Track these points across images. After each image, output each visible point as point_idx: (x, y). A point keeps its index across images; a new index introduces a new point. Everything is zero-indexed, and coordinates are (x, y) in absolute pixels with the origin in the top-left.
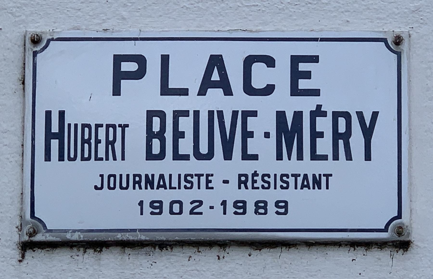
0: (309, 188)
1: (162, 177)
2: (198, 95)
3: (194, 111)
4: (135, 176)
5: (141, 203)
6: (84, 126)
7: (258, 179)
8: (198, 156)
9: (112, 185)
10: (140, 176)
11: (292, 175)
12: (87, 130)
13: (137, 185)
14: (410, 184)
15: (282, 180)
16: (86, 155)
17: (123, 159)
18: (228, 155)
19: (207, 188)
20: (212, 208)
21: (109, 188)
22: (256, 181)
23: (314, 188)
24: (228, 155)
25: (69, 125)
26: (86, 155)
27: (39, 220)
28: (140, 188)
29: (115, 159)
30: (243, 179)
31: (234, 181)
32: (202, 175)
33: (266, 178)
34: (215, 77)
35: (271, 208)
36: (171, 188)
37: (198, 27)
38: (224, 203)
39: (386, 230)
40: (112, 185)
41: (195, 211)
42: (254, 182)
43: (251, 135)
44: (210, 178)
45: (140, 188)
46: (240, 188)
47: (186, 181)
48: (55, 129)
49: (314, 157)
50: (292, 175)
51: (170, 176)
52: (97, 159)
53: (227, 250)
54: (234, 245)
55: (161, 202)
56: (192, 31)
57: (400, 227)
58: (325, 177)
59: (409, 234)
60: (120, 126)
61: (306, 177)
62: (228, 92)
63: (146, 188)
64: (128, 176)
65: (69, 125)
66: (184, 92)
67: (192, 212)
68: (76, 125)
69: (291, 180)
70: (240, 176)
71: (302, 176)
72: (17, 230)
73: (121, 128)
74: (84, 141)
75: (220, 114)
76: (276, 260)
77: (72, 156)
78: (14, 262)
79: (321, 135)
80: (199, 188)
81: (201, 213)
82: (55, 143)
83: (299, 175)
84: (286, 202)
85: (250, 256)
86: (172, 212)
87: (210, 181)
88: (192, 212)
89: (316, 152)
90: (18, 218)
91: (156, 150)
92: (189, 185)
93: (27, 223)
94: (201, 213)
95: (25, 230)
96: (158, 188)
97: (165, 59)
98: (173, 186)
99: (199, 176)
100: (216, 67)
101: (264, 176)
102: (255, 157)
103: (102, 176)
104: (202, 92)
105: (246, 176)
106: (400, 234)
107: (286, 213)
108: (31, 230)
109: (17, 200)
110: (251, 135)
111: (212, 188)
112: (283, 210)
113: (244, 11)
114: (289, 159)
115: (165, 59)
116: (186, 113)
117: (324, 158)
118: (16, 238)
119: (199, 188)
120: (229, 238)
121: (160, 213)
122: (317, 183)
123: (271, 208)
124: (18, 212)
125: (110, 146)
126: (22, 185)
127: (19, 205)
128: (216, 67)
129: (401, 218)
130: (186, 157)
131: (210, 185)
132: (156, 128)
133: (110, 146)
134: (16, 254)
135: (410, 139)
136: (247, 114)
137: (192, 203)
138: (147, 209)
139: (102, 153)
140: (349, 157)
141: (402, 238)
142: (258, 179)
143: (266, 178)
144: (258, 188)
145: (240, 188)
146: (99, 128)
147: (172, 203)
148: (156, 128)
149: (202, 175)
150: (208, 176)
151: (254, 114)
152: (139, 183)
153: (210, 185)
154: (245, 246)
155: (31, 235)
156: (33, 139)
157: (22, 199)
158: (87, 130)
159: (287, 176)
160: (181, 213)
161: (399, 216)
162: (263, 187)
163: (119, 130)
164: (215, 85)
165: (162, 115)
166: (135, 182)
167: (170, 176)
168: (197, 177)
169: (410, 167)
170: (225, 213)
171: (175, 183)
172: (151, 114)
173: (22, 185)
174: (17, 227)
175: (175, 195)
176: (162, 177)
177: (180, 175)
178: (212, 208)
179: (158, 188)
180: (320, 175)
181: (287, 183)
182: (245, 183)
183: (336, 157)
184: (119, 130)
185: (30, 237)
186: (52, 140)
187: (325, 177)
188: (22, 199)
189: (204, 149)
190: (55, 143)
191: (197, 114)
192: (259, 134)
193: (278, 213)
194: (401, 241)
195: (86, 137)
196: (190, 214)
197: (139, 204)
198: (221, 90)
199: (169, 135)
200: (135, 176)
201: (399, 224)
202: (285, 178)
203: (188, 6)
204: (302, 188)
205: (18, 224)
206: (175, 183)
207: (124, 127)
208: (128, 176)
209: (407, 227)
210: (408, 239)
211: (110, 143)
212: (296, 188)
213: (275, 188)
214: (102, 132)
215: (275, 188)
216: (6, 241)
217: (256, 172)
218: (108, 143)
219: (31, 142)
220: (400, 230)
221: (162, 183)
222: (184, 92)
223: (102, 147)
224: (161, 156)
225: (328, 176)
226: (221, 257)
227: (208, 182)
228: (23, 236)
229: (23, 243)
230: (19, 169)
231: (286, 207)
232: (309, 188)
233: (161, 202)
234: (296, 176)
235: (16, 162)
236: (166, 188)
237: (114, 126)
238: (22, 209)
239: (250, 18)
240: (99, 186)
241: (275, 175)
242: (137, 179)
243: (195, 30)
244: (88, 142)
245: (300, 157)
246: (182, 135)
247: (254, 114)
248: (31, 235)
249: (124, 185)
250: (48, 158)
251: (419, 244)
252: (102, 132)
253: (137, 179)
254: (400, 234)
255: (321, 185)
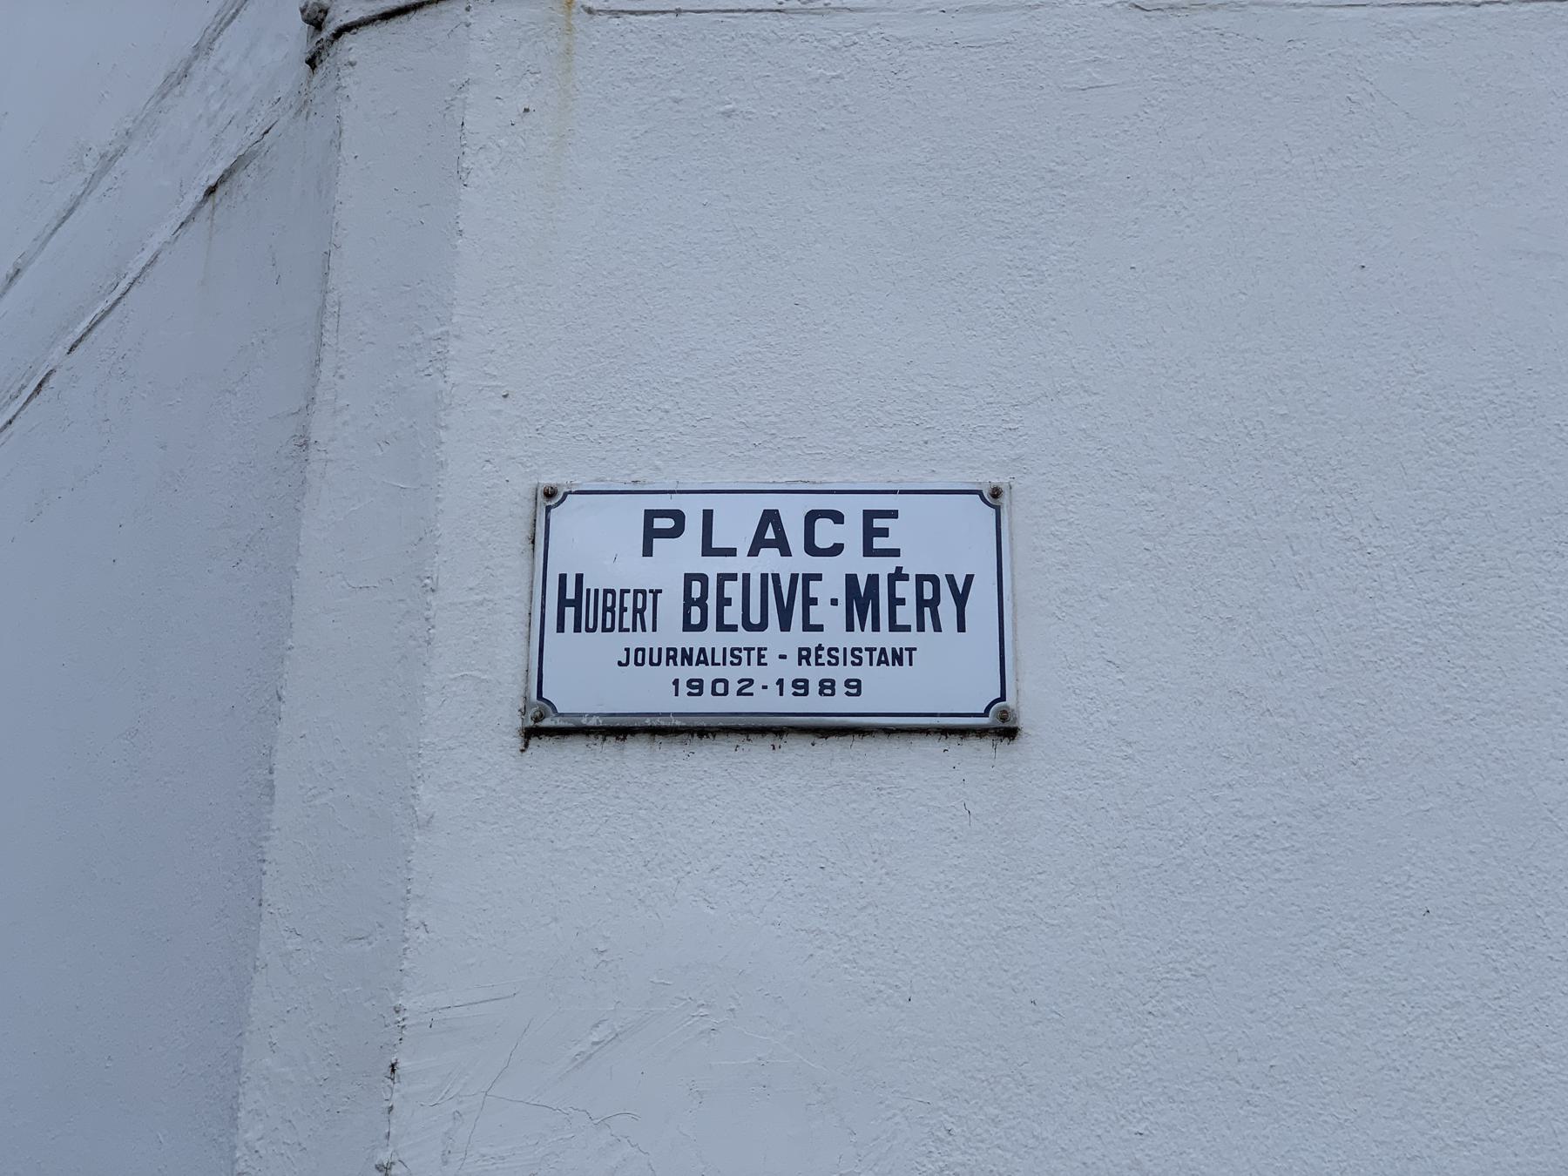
0: (888, 665)
1: (702, 651)
2: (748, 555)
3: (743, 574)
4: (668, 649)
5: (676, 682)
6: (606, 592)
7: (824, 653)
8: (748, 626)
9: (640, 661)
10: (675, 650)
11: (867, 649)
12: (610, 596)
13: (671, 661)
14: (1016, 659)
15: (853, 654)
16: (608, 626)
17: (654, 629)
18: (785, 625)
19: (760, 664)
20: (765, 687)
21: (636, 663)
22: (820, 656)
23: (894, 664)
24: (785, 625)
25: (588, 591)
26: (608, 626)
27: (548, 702)
28: (675, 664)
29: (644, 629)
30: (804, 653)
31: (793, 657)
32: (753, 649)
33: (833, 653)
34: (770, 534)
35: (840, 688)
36: (713, 664)
37: (748, 478)
38: (780, 682)
39: (986, 714)
40: (640, 661)
41: (743, 691)
42: (818, 657)
43: (814, 601)
44: (762, 653)
45: (675, 664)
46: (800, 664)
47: (733, 655)
48: (571, 594)
49: (894, 627)
50: (867, 649)
51: (713, 649)
52: (622, 629)
53: (785, 737)
54: (792, 732)
55: (701, 681)
56: (741, 482)
57: (1004, 711)
58: (908, 652)
59: (1015, 719)
60: (651, 591)
61: (883, 651)
62: (786, 552)
63: (683, 664)
64: (660, 650)
65: (588, 591)
66: (731, 552)
67: (739, 693)
68: (597, 591)
69: (865, 655)
70: (800, 650)
71: (878, 651)
72: (519, 713)
73: (652, 595)
74: (605, 609)
75: (776, 577)
76: (846, 750)
77: (591, 626)
78: (516, 751)
79: (902, 602)
80: (749, 664)
81: (751, 694)
82: (570, 612)
83: (875, 649)
84: (859, 681)
85: (813, 745)
86: (714, 693)
87: (763, 656)
88: (739, 693)
89: (895, 622)
90: (522, 699)
91: (696, 618)
92: (736, 661)
93: (534, 705)
94: (751, 694)
95: (530, 714)
96: (697, 665)
97: (708, 516)
98: (716, 662)
99: (749, 650)
100: (770, 524)
101: (830, 650)
102: (819, 628)
103: (627, 650)
104: (753, 552)
105: (808, 650)
106: (1004, 719)
107: (858, 694)
108: (538, 714)
109: (521, 678)
110: (814, 601)
111: (766, 664)
112: (854, 691)
113: (805, 460)
114: (863, 631)
115: (708, 516)
116: (733, 577)
117: (907, 628)
118: (519, 723)
119: (749, 664)
120: (786, 724)
121: (700, 694)
122: (898, 658)
123: (840, 688)
124: (522, 692)
125: (638, 615)
126: (528, 660)
127: (523, 684)
128: (770, 524)
129: (1005, 700)
130: (733, 628)
131: (763, 661)
132: (696, 594)
133: (638, 615)
134: (518, 742)
135: (1014, 606)
136: (808, 578)
137: (740, 682)
138: (683, 689)
139: (628, 623)
140: (937, 628)
141: (1006, 725)
142: (824, 653)
143: (833, 653)
144: (823, 664)
145: (800, 664)
146: (625, 595)
147: (715, 682)
148: (696, 594)
149: (753, 649)
150: (760, 649)
151: (818, 577)
152: (674, 658)
153: (763, 661)
154: (807, 733)
155: (537, 720)
156: (543, 607)
157: (527, 676)
158: (610, 596)
159: (860, 650)
160: (726, 693)
161: (1003, 698)
162: (829, 663)
163: (650, 597)
164: (770, 544)
165: (703, 579)
166: (668, 658)
167: (713, 649)
168: (746, 652)
169: (1015, 640)
170: (781, 694)
171: (719, 659)
172: (689, 578)
173: (528, 660)
174: (520, 710)
175: (719, 672)
176: (702, 651)
177: (725, 649)
178: (765, 687)
179: (697, 665)
180: (901, 649)
181: (860, 658)
182: (807, 658)
183: (921, 628)
184: (650, 597)
185: (535, 722)
186: (566, 608)
187: (908, 652)
188: (527, 676)
189: (755, 618)
190: (570, 612)
191: (746, 577)
192: (824, 601)
193: (848, 694)
194: (1006, 728)
195: (609, 604)
196: (738, 695)
197: (674, 683)
198: (777, 550)
199: (712, 602)
200: (668, 649)
201: (1003, 707)
202: (857, 653)
203: (736, 454)
204: (878, 665)
205: (522, 706)
206: (719, 659)
207: (656, 593)
208: (660, 650)
209: (1013, 710)
210: (1015, 726)
211: (638, 612)
212: (871, 664)
213: (845, 664)
214: (629, 598)
215: (845, 664)
216: (506, 726)
217: (820, 645)
218: (636, 611)
219: (540, 610)
220: (1004, 715)
221: (702, 658)
222: (731, 552)
223: (628, 616)
224: (702, 626)
225: (911, 650)
226: (777, 747)
227: (760, 657)
228: (527, 721)
229: (526, 729)
230: (524, 642)
231: (859, 687)
232: (888, 665)
233: (701, 681)
234: (871, 650)
235: (521, 633)
236: (707, 665)
237: (644, 592)
238: (526, 689)
239: (813, 467)
240: (624, 661)
241: (845, 649)
242: (672, 653)
243: (745, 482)
244: (612, 610)
245: (876, 628)
246: (729, 602)
247: (818, 577)
248: (537, 720)
249: (655, 660)
250: (561, 628)
251: (1030, 732)
252: (629, 598)
253: (672, 653)
254: (1004, 719)
255: (902, 660)
